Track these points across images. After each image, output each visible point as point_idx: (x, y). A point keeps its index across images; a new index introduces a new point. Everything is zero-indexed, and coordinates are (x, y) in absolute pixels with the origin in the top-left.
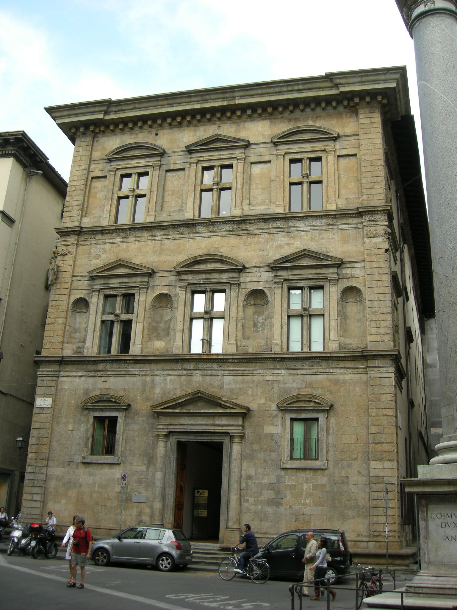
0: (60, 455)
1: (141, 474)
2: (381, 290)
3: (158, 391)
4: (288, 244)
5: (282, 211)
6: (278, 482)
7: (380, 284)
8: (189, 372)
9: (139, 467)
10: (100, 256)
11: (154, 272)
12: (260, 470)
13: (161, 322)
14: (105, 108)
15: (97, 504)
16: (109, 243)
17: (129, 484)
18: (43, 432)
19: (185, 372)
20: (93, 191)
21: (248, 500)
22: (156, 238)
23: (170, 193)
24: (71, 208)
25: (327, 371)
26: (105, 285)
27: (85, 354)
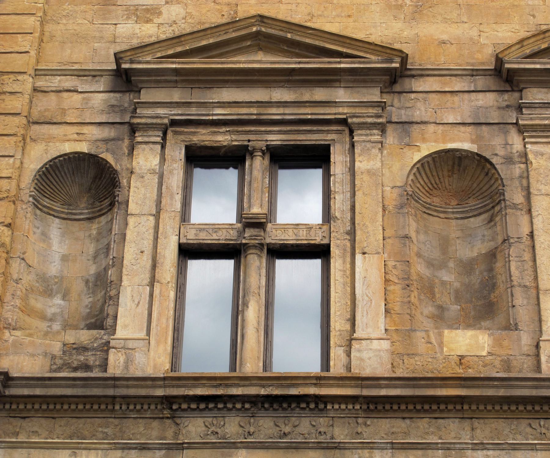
13: (443, 265)
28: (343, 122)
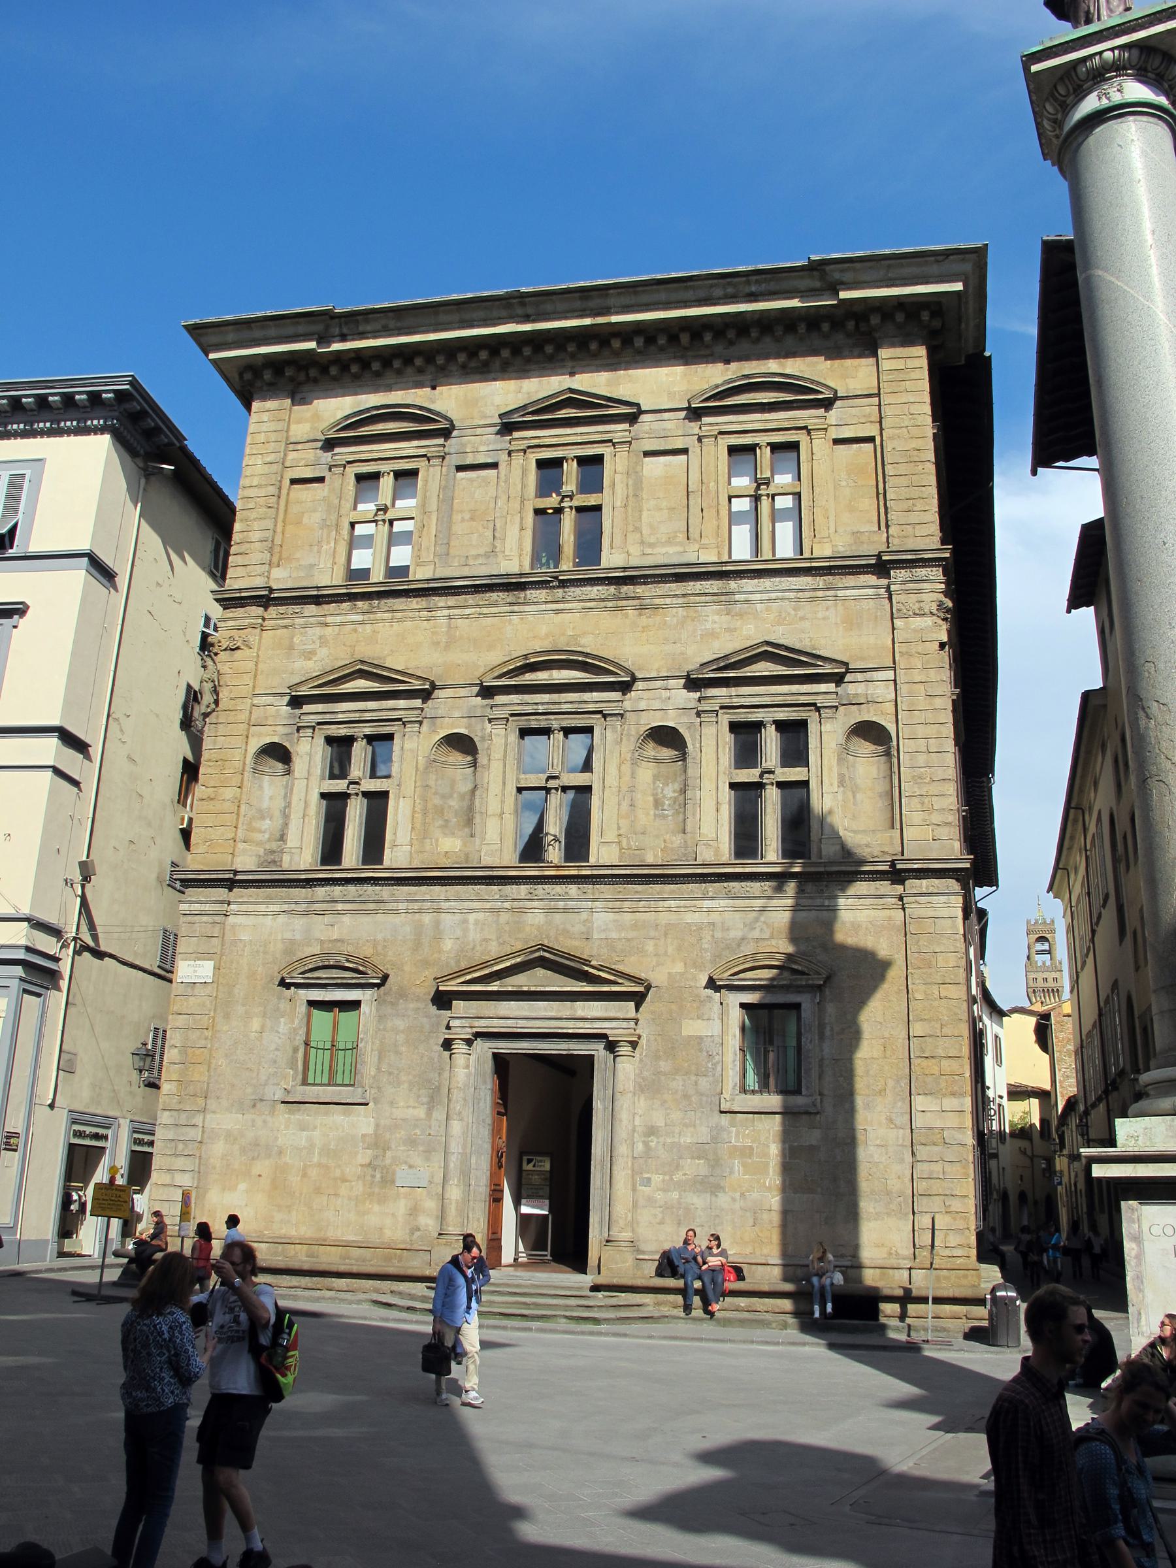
0: (233, 1085)
1: (416, 1126)
2: (931, 731)
3: (448, 945)
4: (729, 630)
5: (715, 559)
6: (715, 1140)
7: (930, 717)
8: (516, 904)
9: (411, 1111)
10: (313, 653)
11: (434, 686)
12: (676, 1115)
13: (451, 796)
14: (319, 328)
15: (318, 1191)
16: (335, 624)
17: (389, 1148)
18: (194, 1035)
19: (507, 905)
20: (294, 509)
21: (649, 1179)
22: (439, 613)
23: (467, 516)
24: (248, 545)
25: (818, 902)
26: (328, 716)
27: (285, 866)
28: (400, 720)
